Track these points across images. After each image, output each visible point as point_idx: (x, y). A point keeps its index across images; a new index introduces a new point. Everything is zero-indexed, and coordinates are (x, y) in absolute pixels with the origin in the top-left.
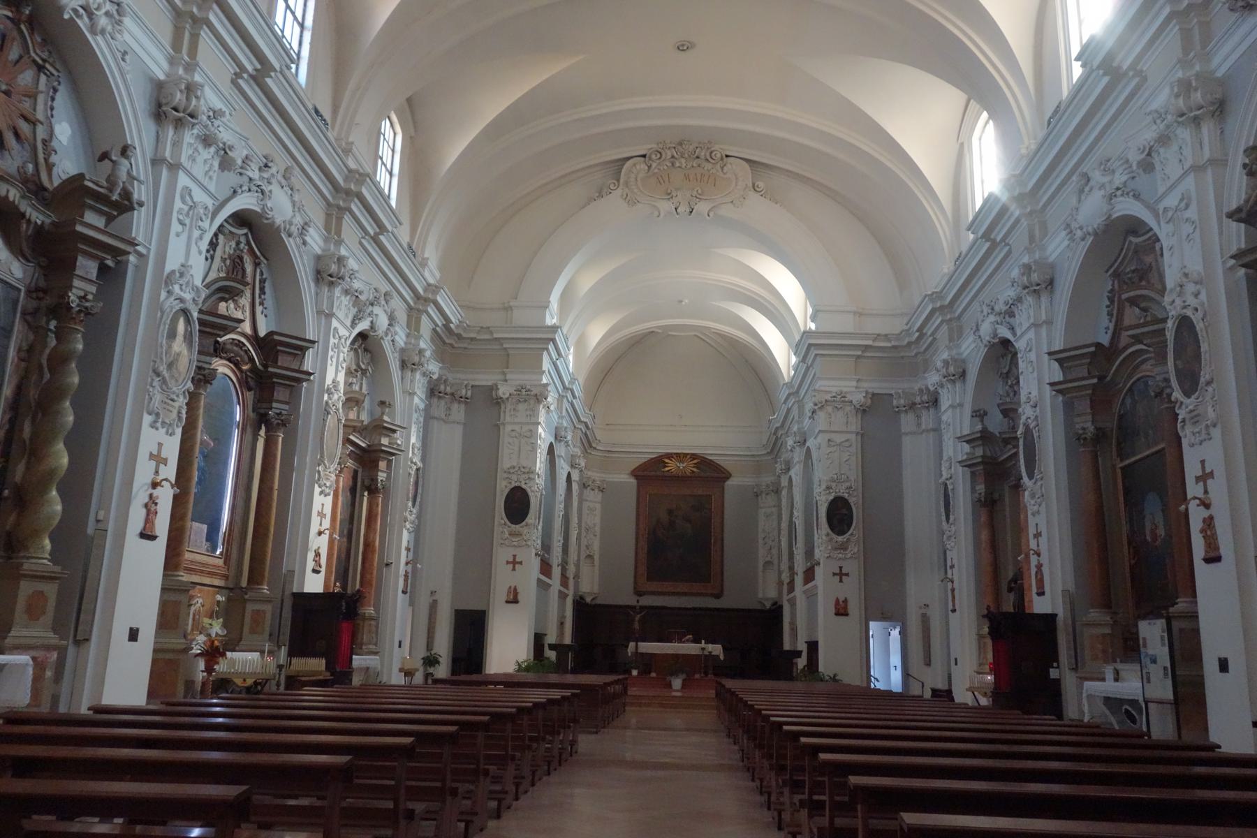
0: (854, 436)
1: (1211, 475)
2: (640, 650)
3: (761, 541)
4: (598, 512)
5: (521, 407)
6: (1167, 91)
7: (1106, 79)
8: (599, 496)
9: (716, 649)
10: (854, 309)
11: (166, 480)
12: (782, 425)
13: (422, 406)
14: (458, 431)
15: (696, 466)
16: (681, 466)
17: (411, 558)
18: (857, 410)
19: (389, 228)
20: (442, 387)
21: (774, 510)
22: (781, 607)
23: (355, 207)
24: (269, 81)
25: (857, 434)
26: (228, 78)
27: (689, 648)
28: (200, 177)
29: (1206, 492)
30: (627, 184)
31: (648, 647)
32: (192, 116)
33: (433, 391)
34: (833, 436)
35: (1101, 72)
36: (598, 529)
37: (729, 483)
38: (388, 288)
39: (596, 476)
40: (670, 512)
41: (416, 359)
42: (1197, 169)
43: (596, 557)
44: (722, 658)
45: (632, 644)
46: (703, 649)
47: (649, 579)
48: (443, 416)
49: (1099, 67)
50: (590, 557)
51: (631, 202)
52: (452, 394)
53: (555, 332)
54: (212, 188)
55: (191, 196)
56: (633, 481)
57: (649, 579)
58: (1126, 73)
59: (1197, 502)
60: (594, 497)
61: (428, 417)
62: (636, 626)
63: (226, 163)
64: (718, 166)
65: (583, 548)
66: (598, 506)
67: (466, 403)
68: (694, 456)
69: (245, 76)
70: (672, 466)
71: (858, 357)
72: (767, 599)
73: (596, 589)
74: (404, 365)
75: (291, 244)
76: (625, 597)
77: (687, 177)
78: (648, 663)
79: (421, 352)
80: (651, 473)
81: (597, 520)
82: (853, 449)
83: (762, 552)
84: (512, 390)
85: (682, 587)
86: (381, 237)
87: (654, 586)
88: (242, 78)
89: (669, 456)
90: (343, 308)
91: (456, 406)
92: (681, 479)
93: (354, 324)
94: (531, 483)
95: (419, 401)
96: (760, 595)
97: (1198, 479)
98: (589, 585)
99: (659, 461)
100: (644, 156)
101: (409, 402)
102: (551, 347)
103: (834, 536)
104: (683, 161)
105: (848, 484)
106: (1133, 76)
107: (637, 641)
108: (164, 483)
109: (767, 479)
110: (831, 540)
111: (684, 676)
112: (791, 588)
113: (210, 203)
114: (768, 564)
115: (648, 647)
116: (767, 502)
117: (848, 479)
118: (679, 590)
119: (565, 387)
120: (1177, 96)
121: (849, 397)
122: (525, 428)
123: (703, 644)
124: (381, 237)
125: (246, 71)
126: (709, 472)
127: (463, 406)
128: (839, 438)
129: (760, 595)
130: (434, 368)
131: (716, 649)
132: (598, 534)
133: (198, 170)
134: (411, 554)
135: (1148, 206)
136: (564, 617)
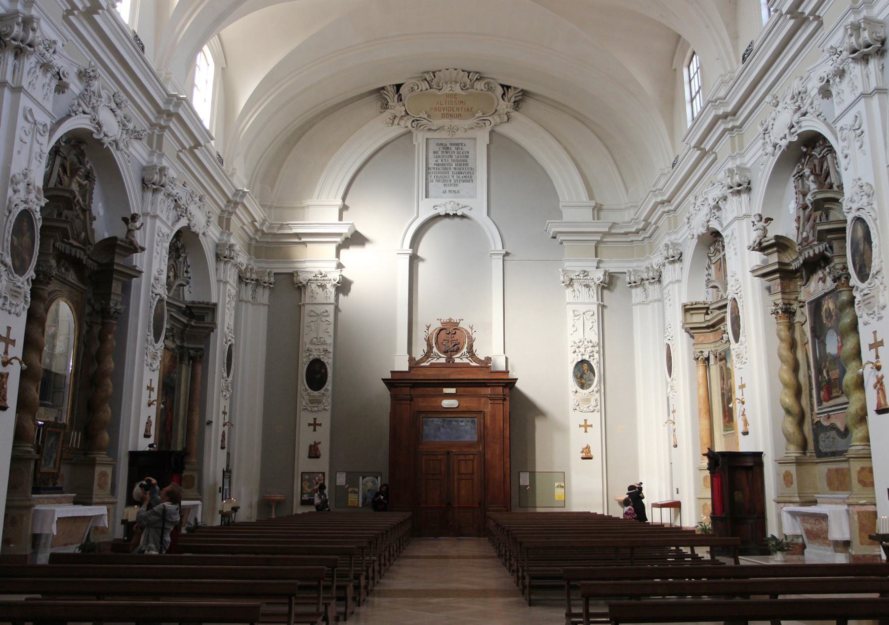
1: (881, 343)
6: (842, 30)
7: (792, 22)
11: (15, 358)
13: (233, 292)
14: (264, 311)
17: (227, 421)
19: (202, 143)
20: (248, 275)
23: (173, 125)
24: (96, 17)
26: (60, 13)
28: (39, 99)
29: (877, 357)
32: (30, 45)
33: (241, 279)
35: (789, 16)
38: (201, 192)
41: (227, 253)
42: (863, 95)
48: (250, 299)
49: (787, 13)
52: (257, 280)
54: (49, 108)
55: (32, 116)
58: (807, 19)
59: (871, 365)
61: (240, 300)
63: (61, 88)
67: (270, 288)
69: (76, 12)
74: (218, 257)
75: (118, 156)
79: (231, 246)
86: (196, 151)
88: (73, 14)
90: (162, 207)
91: (260, 290)
93: (174, 224)
95: (232, 288)
97: (871, 346)
101: (223, 290)
106: (814, 20)
108: (13, 361)
113: (48, 121)
120: (851, 35)
124: (196, 151)
125: (77, 9)
127: (267, 292)
130: (242, 259)
133: (38, 94)
134: (227, 417)
135: (828, 125)
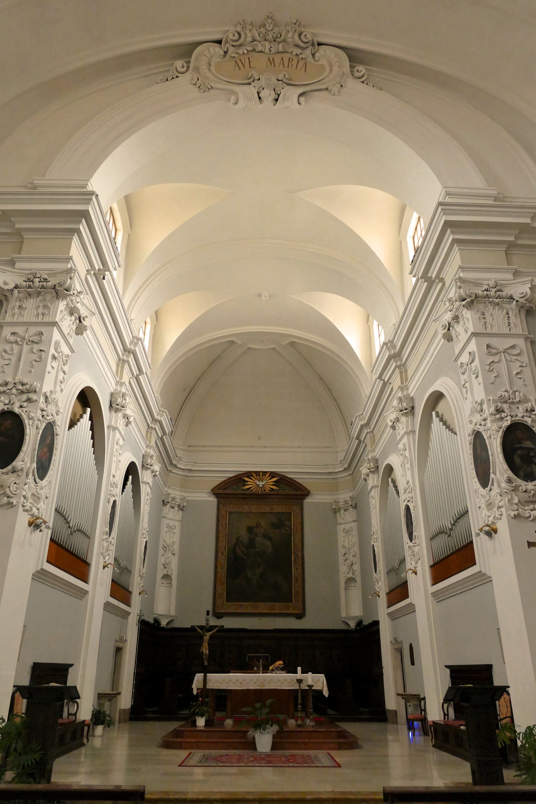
0: (521, 343)
2: (210, 686)
3: (341, 559)
4: (177, 531)
5: (30, 303)
8: (179, 515)
9: (317, 681)
10: (495, 193)
12: (367, 424)
15: (276, 483)
16: (261, 484)
18: (521, 307)
21: (353, 525)
22: (376, 623)
25: (526, 339)
27: (278, 679)
30: (197, 69)
31: (220, 681)
34: (494, 342)
36: (176, 547)
37: (308, 501)
39: (176, 493)
40: (250, 530)
43: (174, 577)
44: (326, 693)
45: (199, 677)
46: (300, 681)
47: (229, 599)
50: (166, 577)
51: (204, 88)
53: (88, 201)
56: (213, 500)
57: (229, 599)
60: (172, 516)
62: (205, 650)
64: (308, 52)
65: (160, 566)
66: (177, 524)
68: (273, 474)
70: (252, 484)
71: (510, 246)
72: (352, 618)
73: (173, 613)
76: (197, 616)
77: (272, 62)
78: (222, 698)
80: (232, 491)
81: (176, 538)
82: (525, 359)
83: (343, 569)
84: (20, 281)
85: (262, 607)
87: (231, 607)
89: (249, 474)
92: (262, 497)
94: (29, 407)
96: (343, 615)
98: (165, 607)
99: (239, 479)
100: (219, 42)
102: (83, 227)
103: (519, 481)
104: (267, 44)
105: (529, 405)
107: (206, 671)
109: (344, 496)
110: (515, 489)
111: (275, 728)
112: (399, 592)
114: (350, 580)
115: (220, 681)
116: (347, 518)
117: (527, 400)
118: (260, 610)
119: (126, 350)
121: (507, 291)
122: (33, 330)
123: (299, 675)
126: (290, 491)
128: (502, 344)
129: (343, 615)
131: (317, 681)
132: (177, 552)
136: (122, 640)
